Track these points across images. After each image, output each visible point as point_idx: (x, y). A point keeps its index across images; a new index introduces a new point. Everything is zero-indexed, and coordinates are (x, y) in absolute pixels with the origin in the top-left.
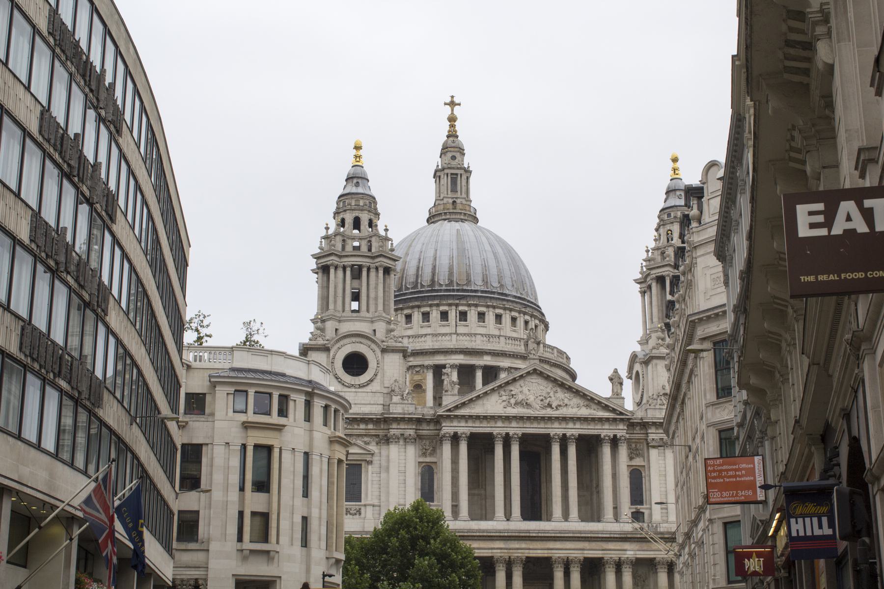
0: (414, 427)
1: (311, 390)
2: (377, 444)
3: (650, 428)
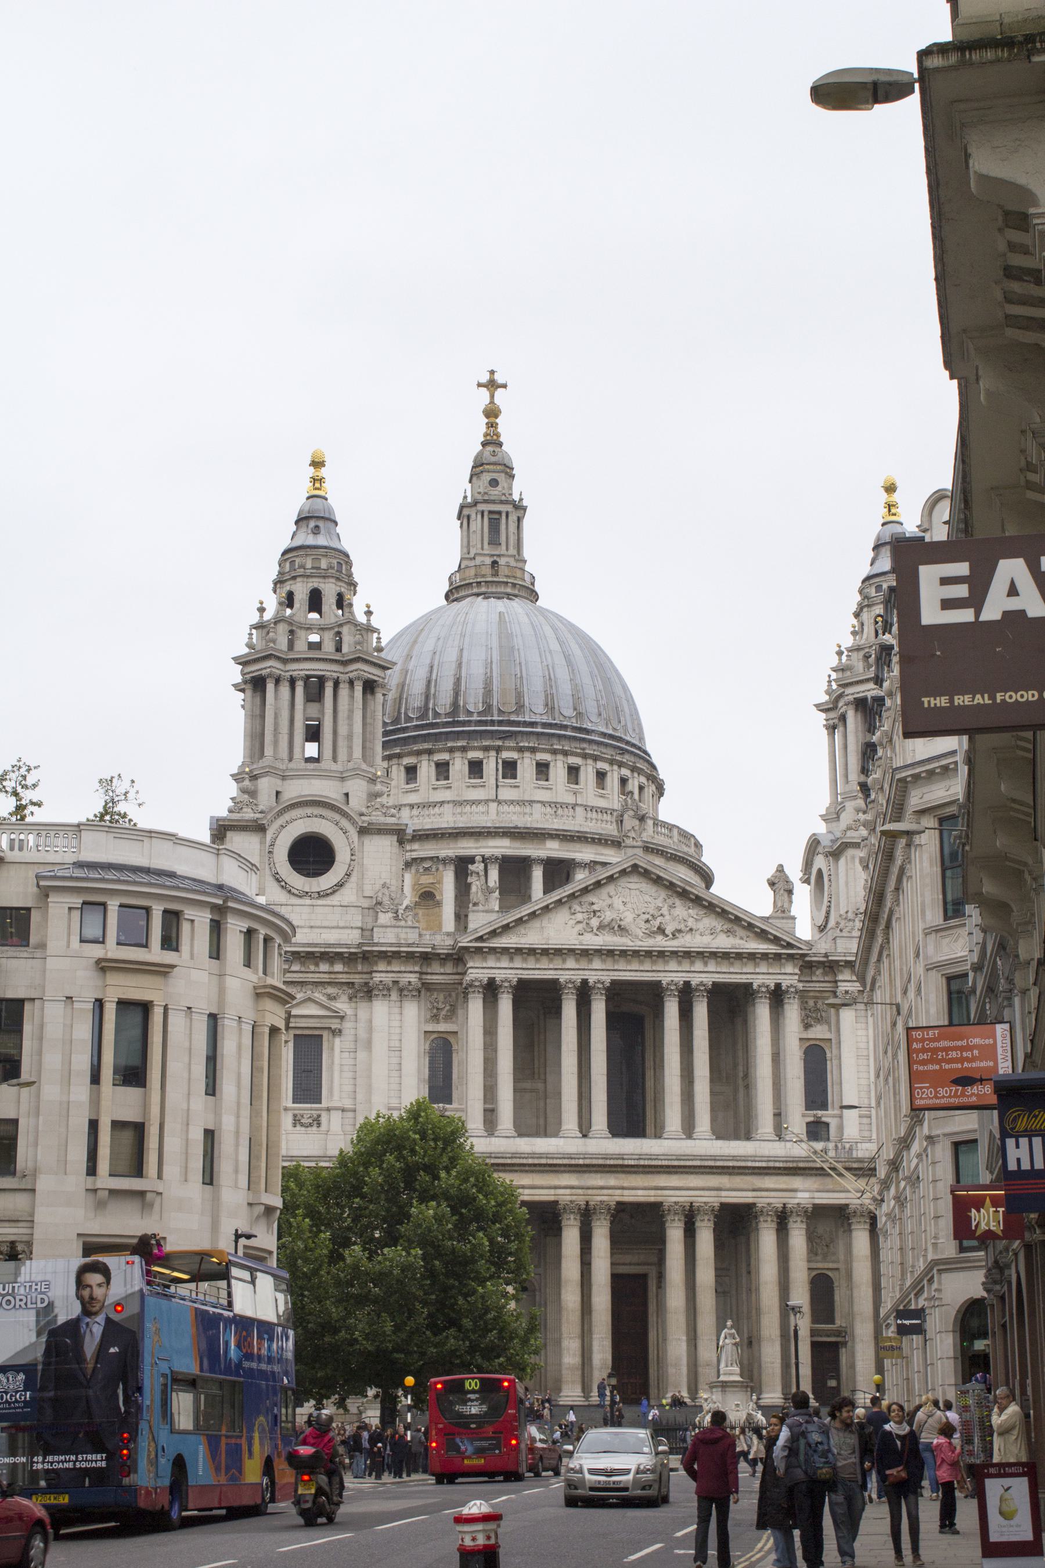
0: (417, 969)
1: (220, 902)
2: (350, 999)
3: (842, 972)
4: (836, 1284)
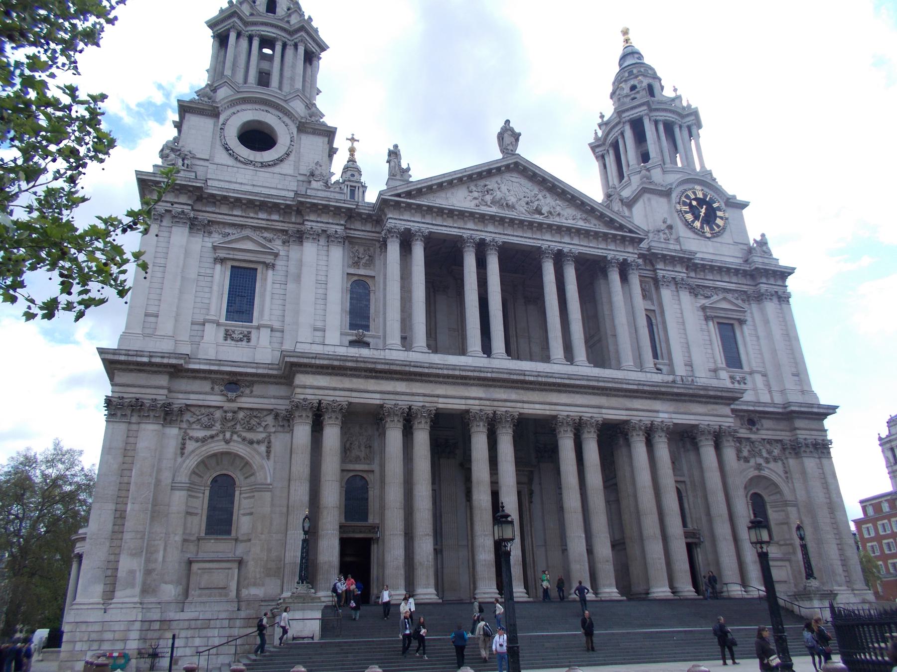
0: (342, 222)
2: (284, 243)
4: (684, 494)
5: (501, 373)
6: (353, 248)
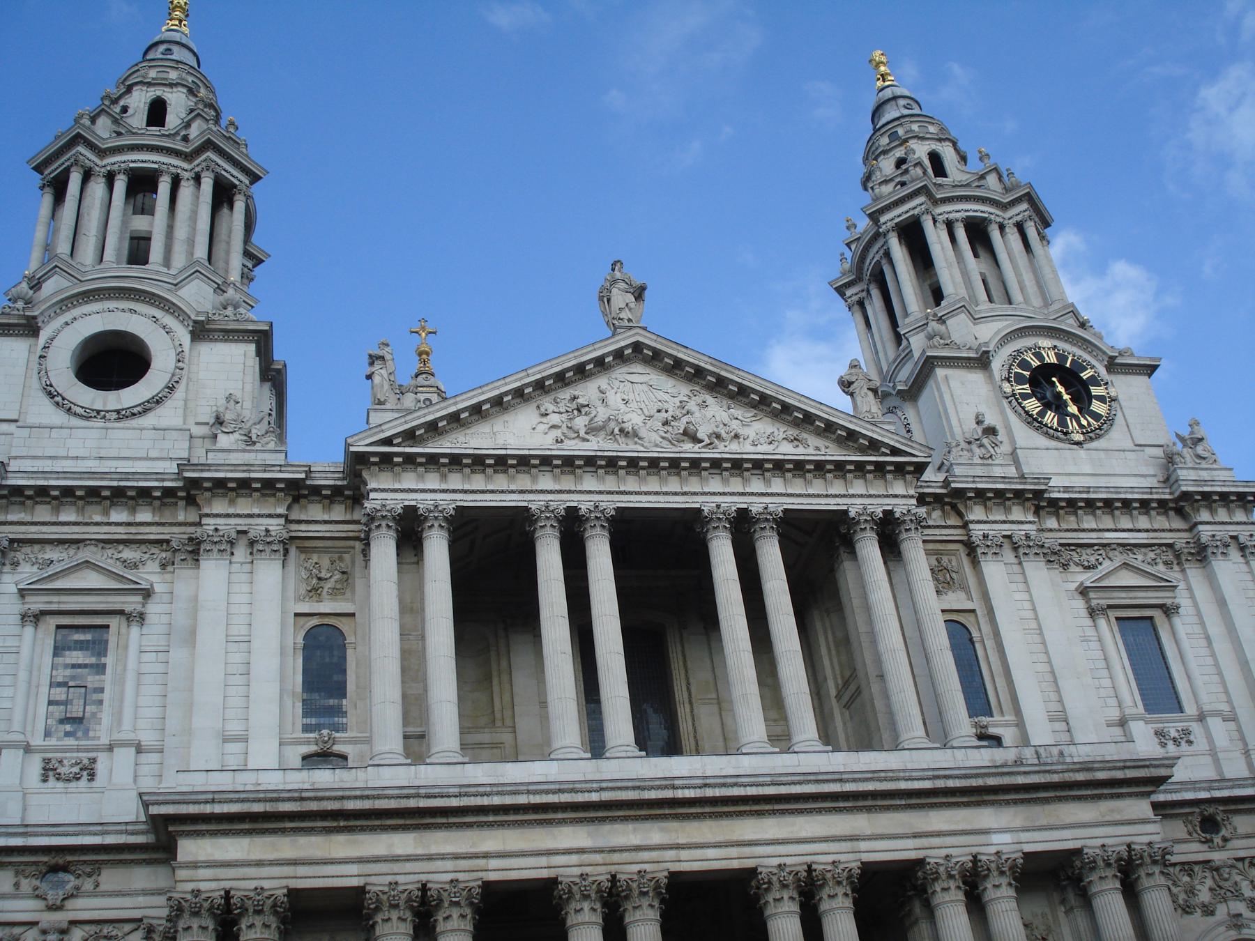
2: (163, 566)
5: (620, 788)
6: (306, 560)
